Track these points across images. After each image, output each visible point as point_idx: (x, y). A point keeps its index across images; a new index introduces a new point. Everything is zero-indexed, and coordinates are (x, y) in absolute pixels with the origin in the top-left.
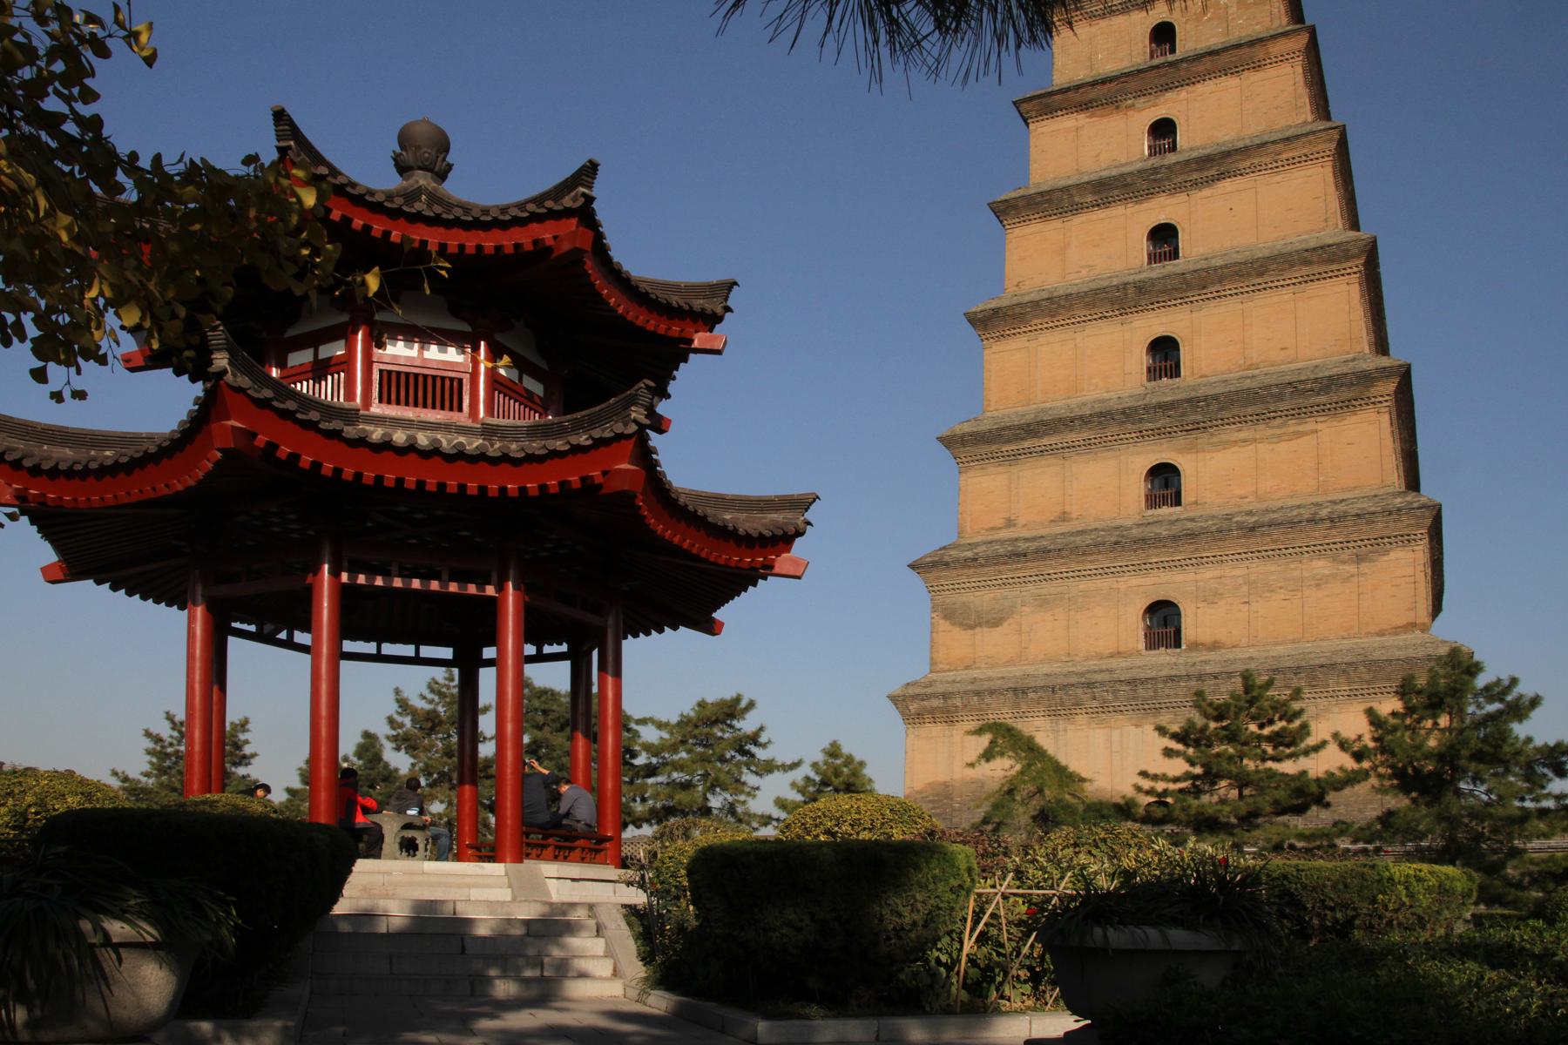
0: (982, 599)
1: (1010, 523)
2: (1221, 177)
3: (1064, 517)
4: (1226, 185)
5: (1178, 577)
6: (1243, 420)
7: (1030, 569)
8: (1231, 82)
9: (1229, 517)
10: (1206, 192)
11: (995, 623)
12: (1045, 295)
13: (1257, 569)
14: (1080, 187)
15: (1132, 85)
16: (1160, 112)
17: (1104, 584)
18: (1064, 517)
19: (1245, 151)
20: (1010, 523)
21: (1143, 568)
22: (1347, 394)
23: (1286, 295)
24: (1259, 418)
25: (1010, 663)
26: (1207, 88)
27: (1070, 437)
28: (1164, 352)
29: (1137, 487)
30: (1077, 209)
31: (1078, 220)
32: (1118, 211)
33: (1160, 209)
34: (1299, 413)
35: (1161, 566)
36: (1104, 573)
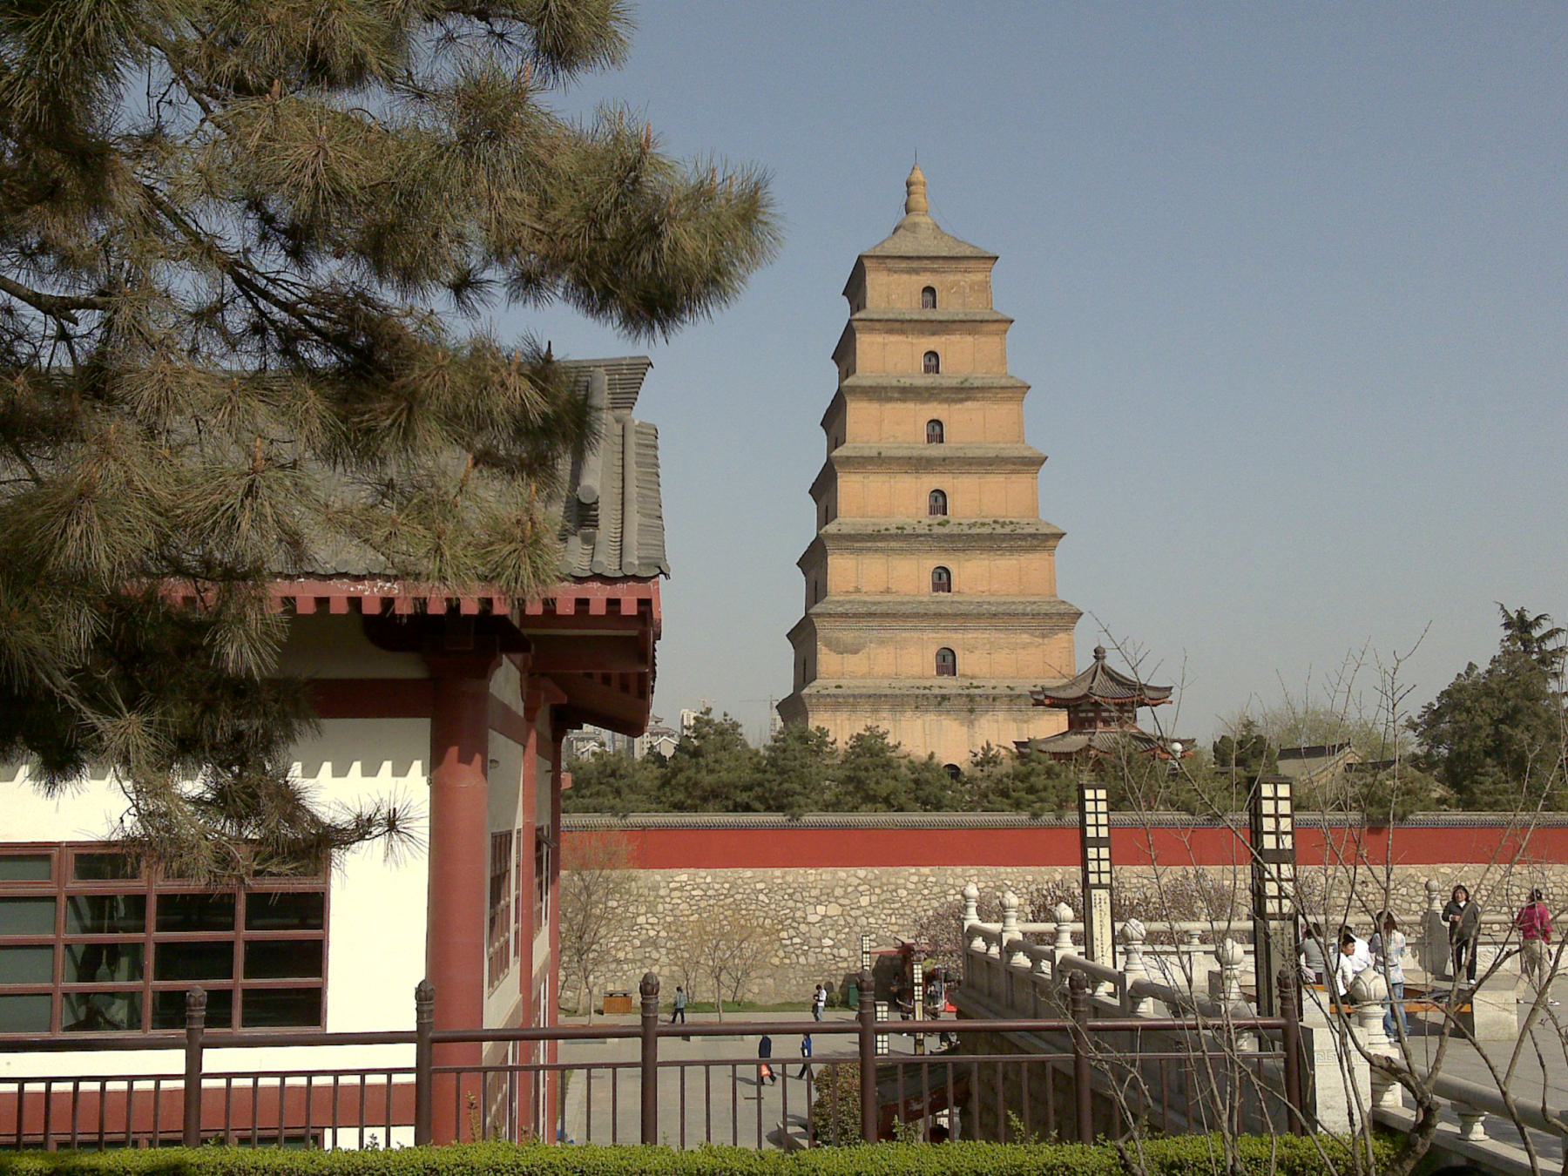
0: (847, 636)
1: (857, 590)
2: (967, 399)
3: (888, 591)
4: (969, 404)
5: (954, 635)
6: (982, 550)
7: (875, 623)
8: (969, 339)
9: (980, 604)
10: (959, 406)
11: (856, 652)
12: (874, 453)
13: (994, 635)
14: (893, 388)
15: (919, 326)
16: (932, 348)
17: (916, 635)
18: (888, 591)
19: (981, 389)
20: (857, 590)
21: (934, 630)
22: (1035, 543)
23: (1001, 478)
24: (991, 549)
25: (863, 677)
26: (956, 338)
27: (893, 544)
28: (939, 501)
29: (927, 581)
30: (890, 400)
31: (889, 406)
32: (911, 406)
33: (936, 410)
34: (1012, 550)
35: (945, 628)
36: (915, 629)
